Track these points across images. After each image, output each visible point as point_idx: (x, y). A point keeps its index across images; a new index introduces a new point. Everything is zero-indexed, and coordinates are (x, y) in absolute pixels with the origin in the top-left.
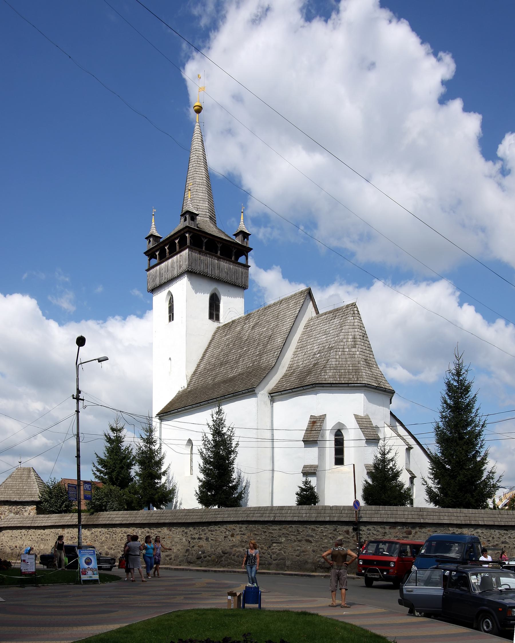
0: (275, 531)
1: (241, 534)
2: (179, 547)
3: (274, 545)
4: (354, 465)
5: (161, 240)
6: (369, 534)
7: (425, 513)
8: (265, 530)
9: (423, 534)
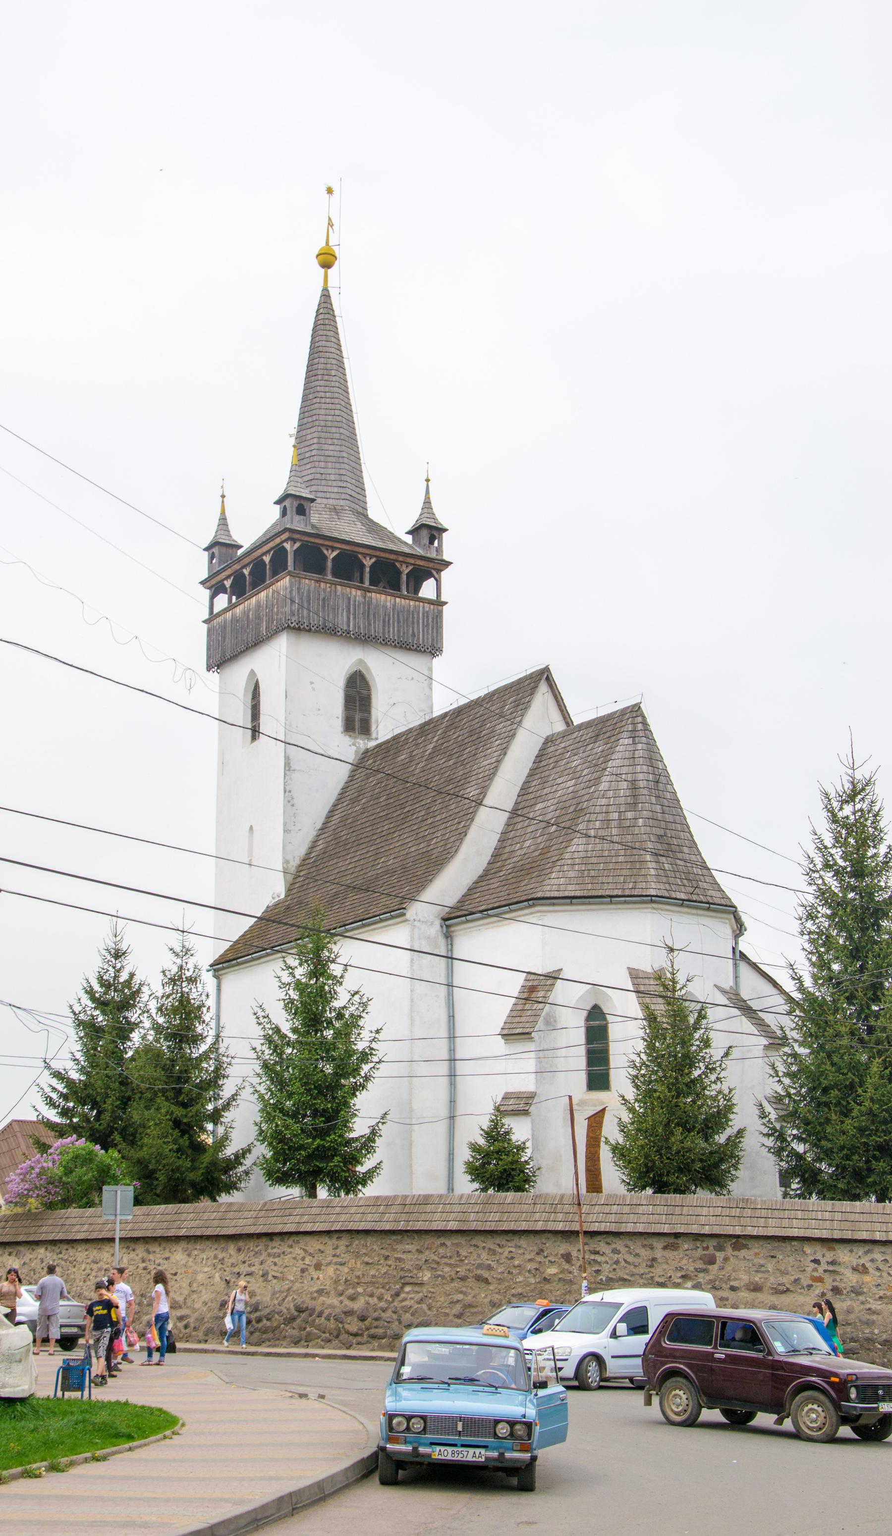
0: (409, 1256)
1: (336, 1263)
3: (407, 1289)
4: (570, 1097)
5: (240, 552)
6: (617, 1262)
8: (387, 1254)
9: (743, 1264)
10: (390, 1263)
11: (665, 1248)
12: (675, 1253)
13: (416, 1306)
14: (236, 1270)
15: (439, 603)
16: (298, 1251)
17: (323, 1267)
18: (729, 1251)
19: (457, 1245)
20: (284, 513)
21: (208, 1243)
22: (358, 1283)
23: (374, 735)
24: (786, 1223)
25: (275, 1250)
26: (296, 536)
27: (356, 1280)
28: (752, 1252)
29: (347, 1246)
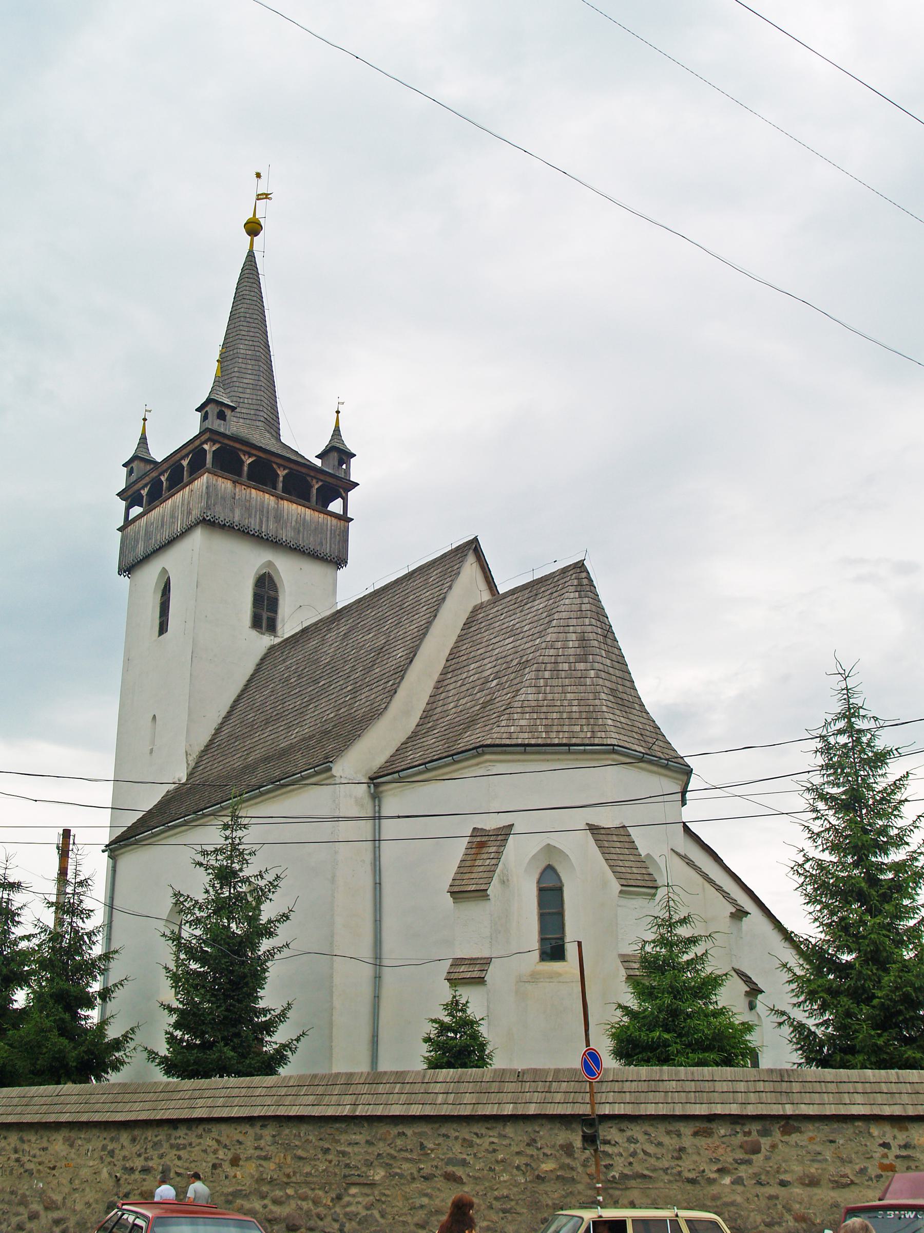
0: (356, 1149)
1: (259, 1157)
2: (90, 1196)
3: (353, 1190)
4: (580, 944)
6: (634, 1154)
7: (796, 1087)
8: (327, 1146)
10: (330, 1157)
11: (695, 1134)
12: (709, 1140)
13: (364, 1213)
14: (129, 1164)
15: (345, 518)
16: (209, 1142)
17: (241, 1163)
18: (777, 1135)
19: (421, 1134)
20: (205, 418)
21: (96, 1132)
22: (287, 1184)
23: (279, 632)
24: (846, 1098)
25: (181, 1141)
26: (216, 437)
27: (285, 1180)
28: (805, 1137)
29: (274, 1136)
